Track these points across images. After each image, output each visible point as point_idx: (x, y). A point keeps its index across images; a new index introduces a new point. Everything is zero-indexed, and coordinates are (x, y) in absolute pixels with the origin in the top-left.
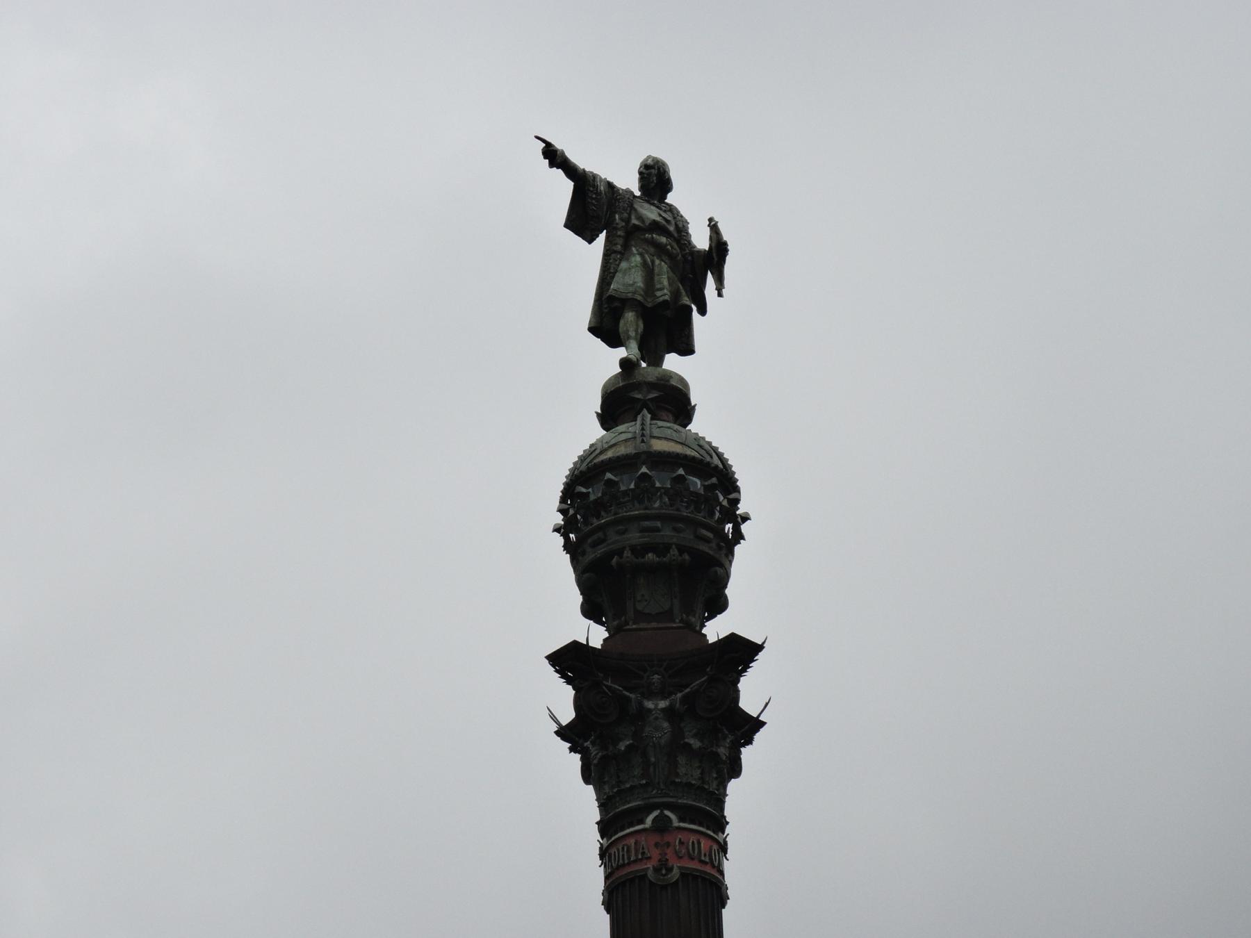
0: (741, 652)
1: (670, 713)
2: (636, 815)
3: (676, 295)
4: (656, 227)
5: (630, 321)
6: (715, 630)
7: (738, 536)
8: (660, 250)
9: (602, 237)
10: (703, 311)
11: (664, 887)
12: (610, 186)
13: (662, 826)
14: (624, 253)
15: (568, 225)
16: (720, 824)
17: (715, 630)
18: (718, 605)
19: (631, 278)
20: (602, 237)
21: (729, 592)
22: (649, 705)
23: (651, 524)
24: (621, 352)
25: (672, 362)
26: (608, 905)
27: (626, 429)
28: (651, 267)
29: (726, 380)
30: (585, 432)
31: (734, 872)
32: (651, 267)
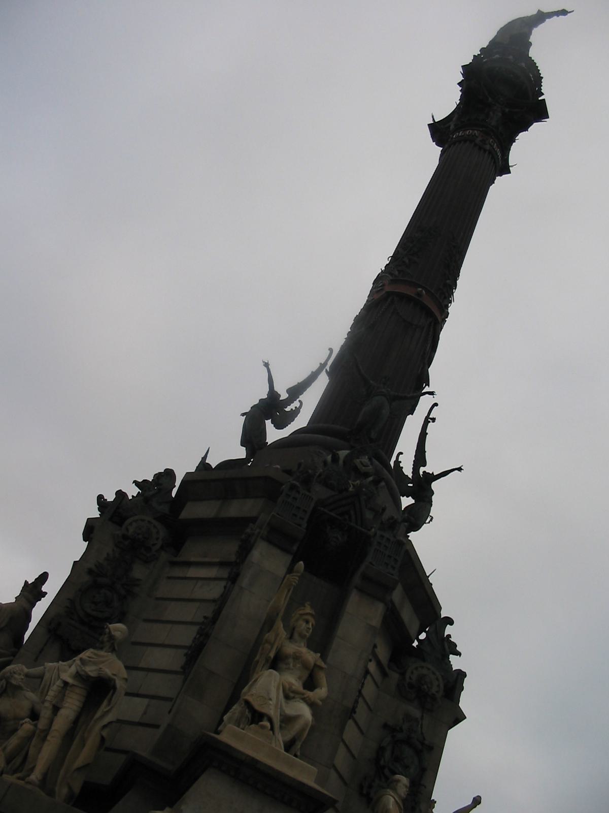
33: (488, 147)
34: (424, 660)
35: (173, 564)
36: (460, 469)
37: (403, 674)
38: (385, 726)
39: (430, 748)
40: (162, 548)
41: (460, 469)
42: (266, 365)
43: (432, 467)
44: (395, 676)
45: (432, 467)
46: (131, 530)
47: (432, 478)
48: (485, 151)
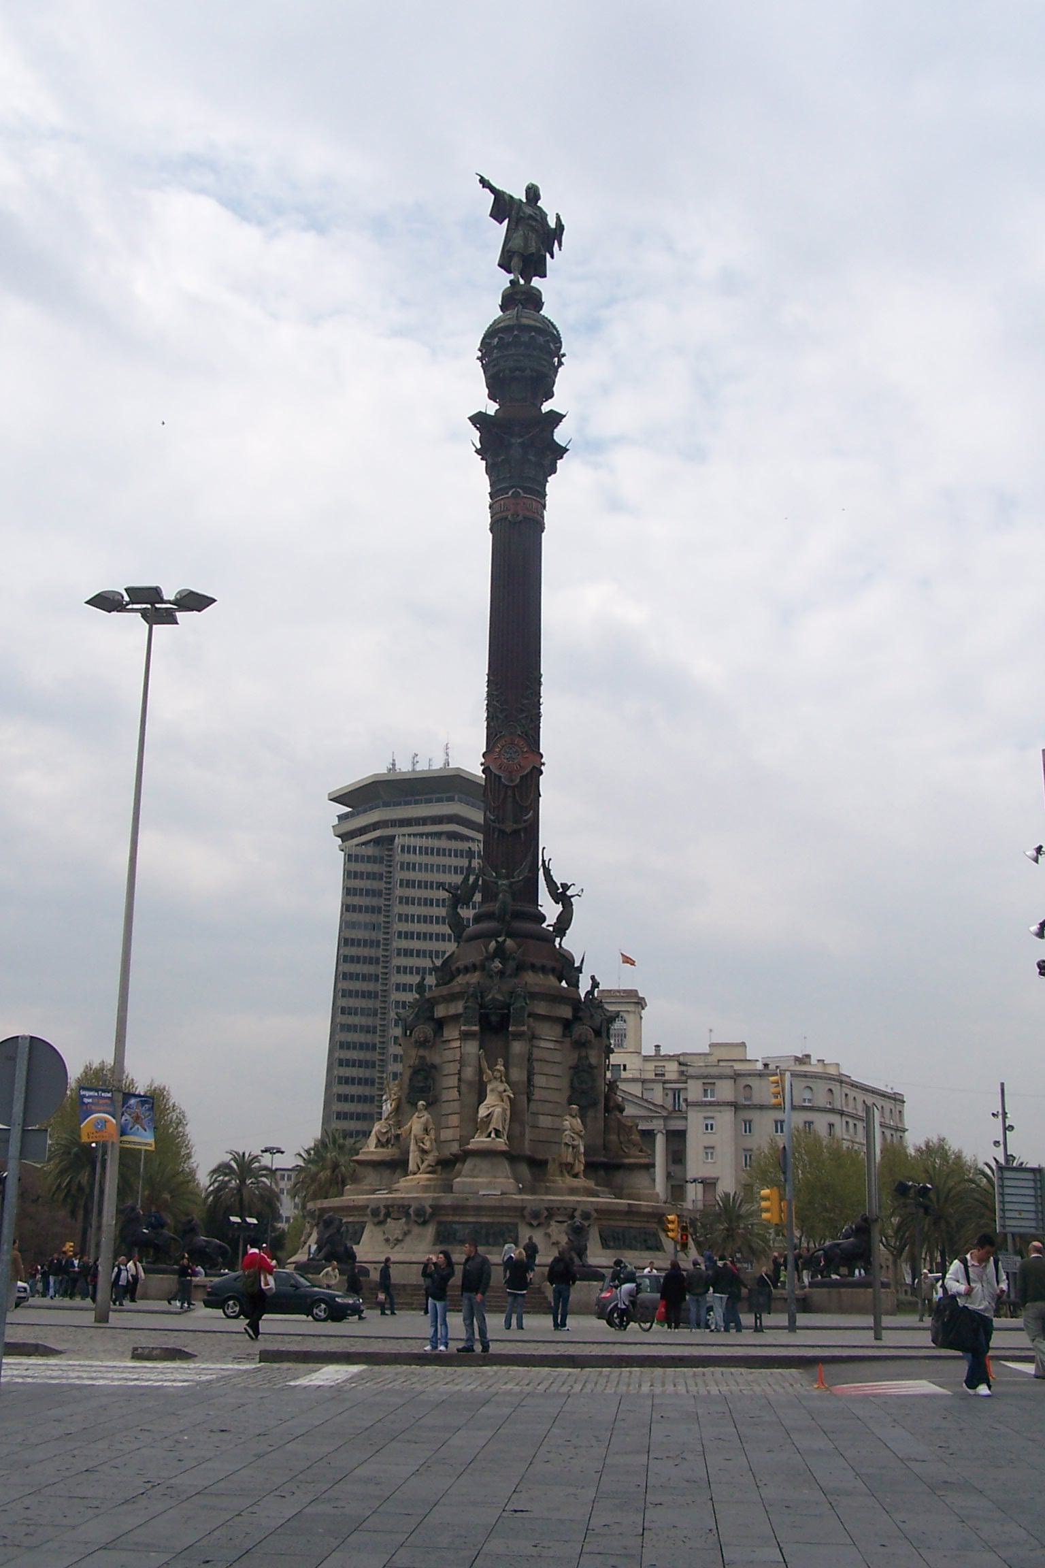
0: (556, 418)
1: (522, 444)
2: (505, 491)
3: (539, 250)
4: (530, 217)
5: (515, 262)
6: (546, 407)
7: (561, 363)
8: (533, 229)
9: (506, 221)
10: (552, 257)
12: (511, 197)
13: (516, 495)
14: (516, 229)
15: (491, 215)
16: (543, 495)
17: (546, 407)
18: (550, 395)
19: (517, 242)
20: (506, 221)
21: (555, 389)
22: (513, 441)
23: (521, 357)
24: (512, 276)
25: (536, 282)
26: (491, 530)
27: (512, 313)
28: (529, 236)
29: (558, 292)
30: (492, 312)
31: (549, 516)
32: (529, 236)
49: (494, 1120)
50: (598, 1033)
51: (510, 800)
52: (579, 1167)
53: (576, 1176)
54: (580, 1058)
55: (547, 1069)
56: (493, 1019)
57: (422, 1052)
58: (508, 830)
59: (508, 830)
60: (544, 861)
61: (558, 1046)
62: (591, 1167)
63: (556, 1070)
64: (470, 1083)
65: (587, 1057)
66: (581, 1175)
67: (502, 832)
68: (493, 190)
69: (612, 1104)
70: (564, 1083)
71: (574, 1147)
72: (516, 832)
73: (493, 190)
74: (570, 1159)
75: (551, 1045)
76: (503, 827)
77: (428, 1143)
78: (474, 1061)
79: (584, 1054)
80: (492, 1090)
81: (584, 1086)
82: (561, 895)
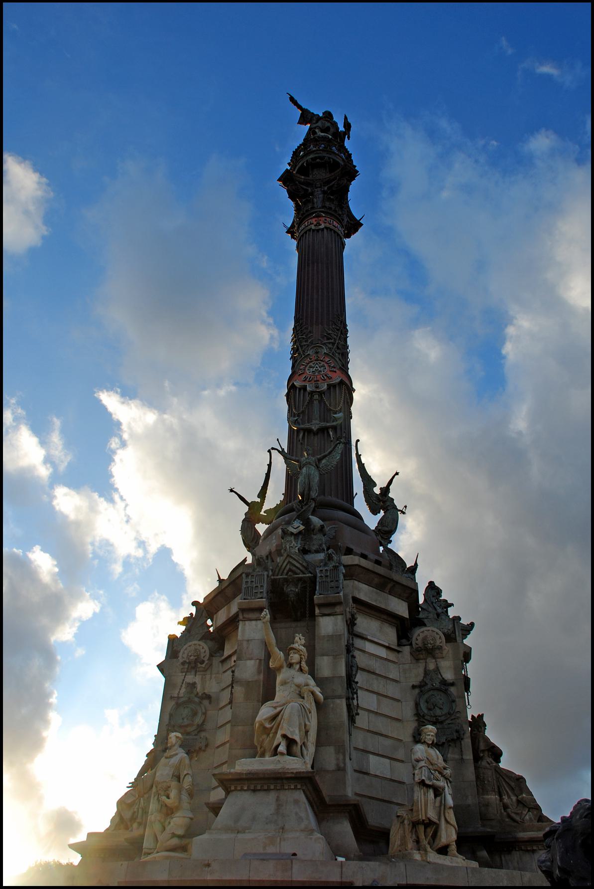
11: (318, 231)
33: (322, 226)
34: (425, 625)
35: (223, 662)
36: (397, 474)
37: (411, 644)
38: (414, 687)
39: (452, 684)
40: (211, 655)
41: (397, 474)
42: (231, 491)
43: (380, 483)
44: (406, 650)
45: (380, 483)
46: (185, 656)
47: (386, 490)
48: (322, 230)
49: (284, 725)
50: (450, 638)
51: (316, 403)
52: (448, 834)
53: (443, 851)
54: (426, 672)
55: (378, 685)
56: (292, 590)
57: (190, 678)
58: (315, 428)
59: (315, 428)
60: (358, 457)
61: (392, 656)
62: (467, 844)
63: (392, 690)
64: (247, 684)
65: (437, 670)
66: (454, 847)
67: (309, 431)
68: (300, 107)
69: (482, 746)
70: (407, 710)
71: (438, 792)
72: (323, 430)
73: (300, 107)
74: (432, 815)
75: (383, 653)
76: (307, 426)
77: (173, 794)
78: (259, 653)
79: (431, 666)
80: (284, 683)
81: (438, 712)
82: (381, 501)
